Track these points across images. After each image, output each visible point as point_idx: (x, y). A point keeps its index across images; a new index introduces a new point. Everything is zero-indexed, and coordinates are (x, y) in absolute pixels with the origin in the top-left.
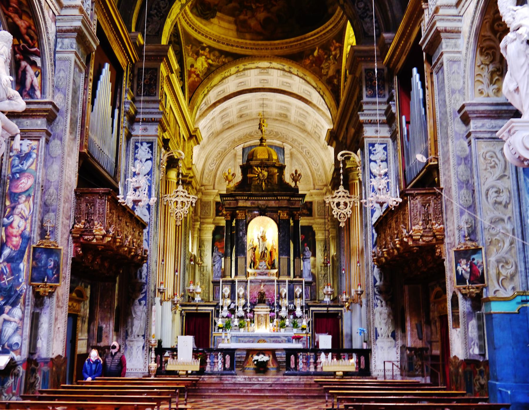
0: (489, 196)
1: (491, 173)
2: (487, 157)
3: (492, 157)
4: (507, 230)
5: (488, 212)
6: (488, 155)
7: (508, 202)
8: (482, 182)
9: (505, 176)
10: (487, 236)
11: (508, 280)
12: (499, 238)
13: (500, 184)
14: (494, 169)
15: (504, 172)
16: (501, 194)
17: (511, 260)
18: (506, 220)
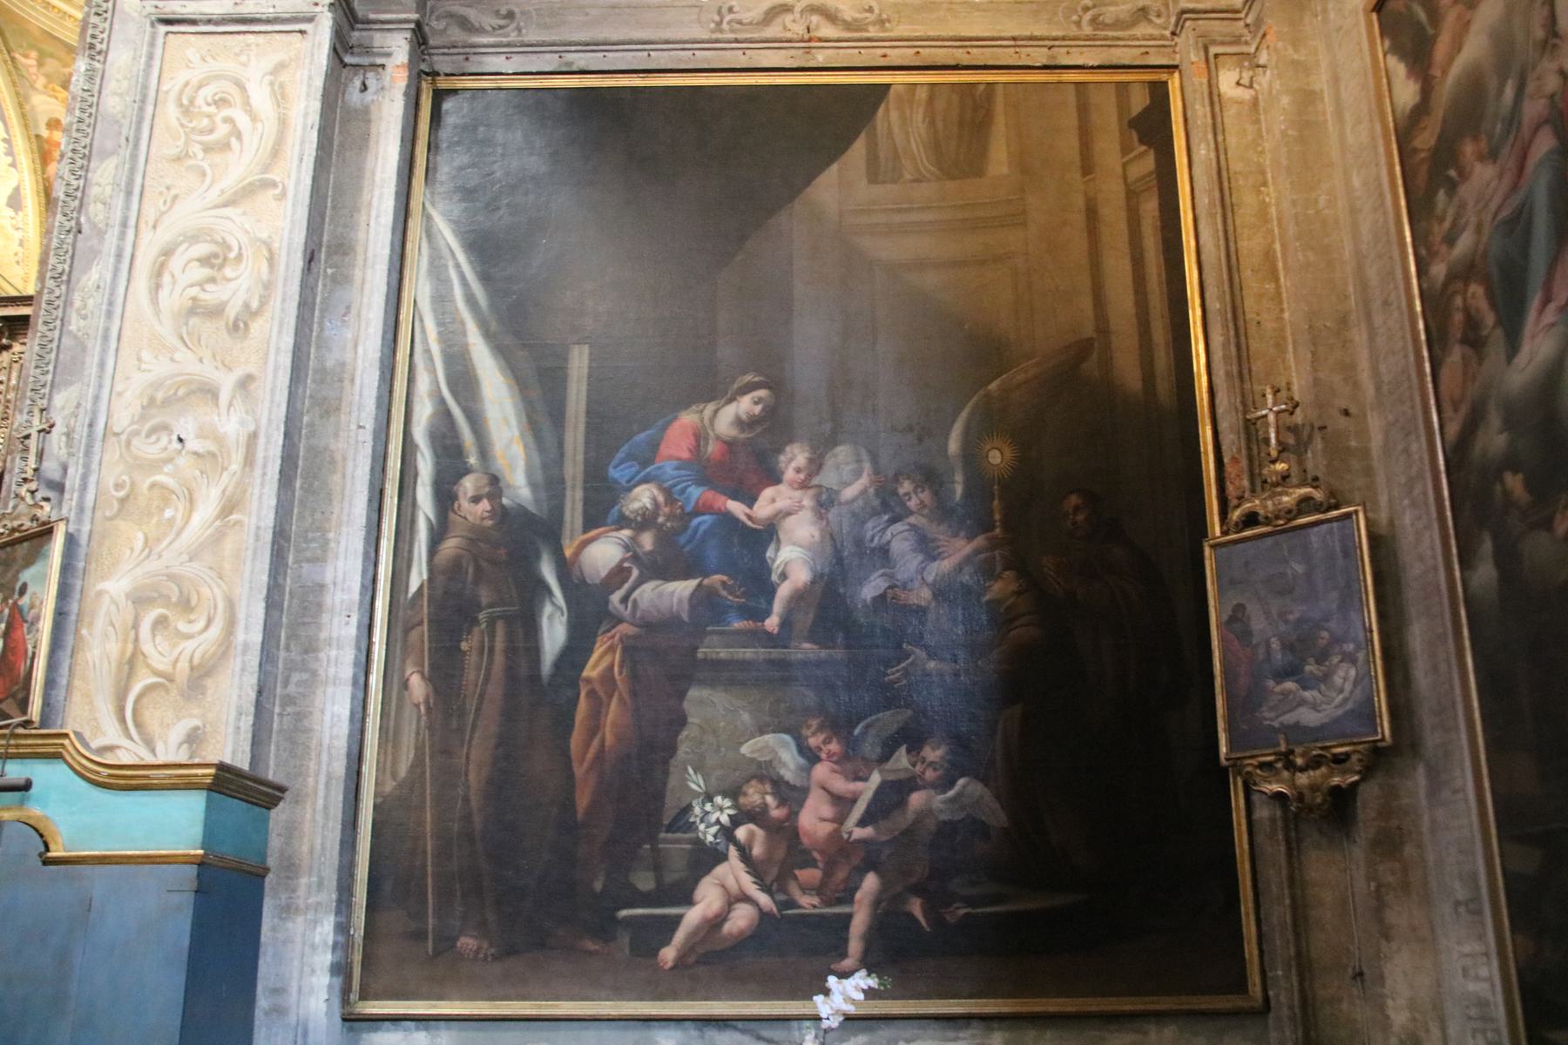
0: (166, 278)
1: (204, 174)
2: (200, 101)
3: (221, 102)
4: (219, 439)
5: (145, 355)
6: (208, 92)
7: (255, 305)
8: (150, 213)
9: (274, 184)
10: (111, 470)
11: (174, 692)
12: (171, 482)
13: (238, 226)
14: (217, 158)
15: (266, 168)
16: (228, 272)
17: (211, 593)
18: (224, 397)
